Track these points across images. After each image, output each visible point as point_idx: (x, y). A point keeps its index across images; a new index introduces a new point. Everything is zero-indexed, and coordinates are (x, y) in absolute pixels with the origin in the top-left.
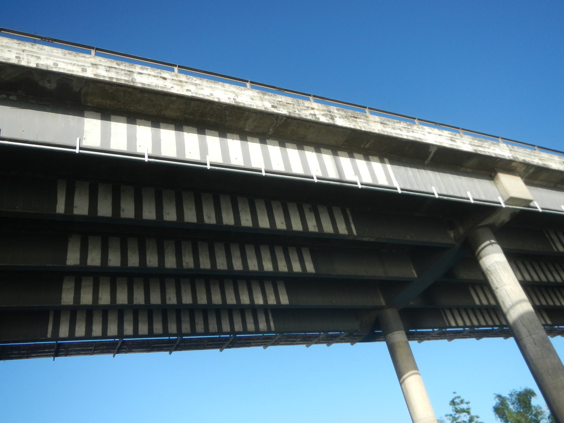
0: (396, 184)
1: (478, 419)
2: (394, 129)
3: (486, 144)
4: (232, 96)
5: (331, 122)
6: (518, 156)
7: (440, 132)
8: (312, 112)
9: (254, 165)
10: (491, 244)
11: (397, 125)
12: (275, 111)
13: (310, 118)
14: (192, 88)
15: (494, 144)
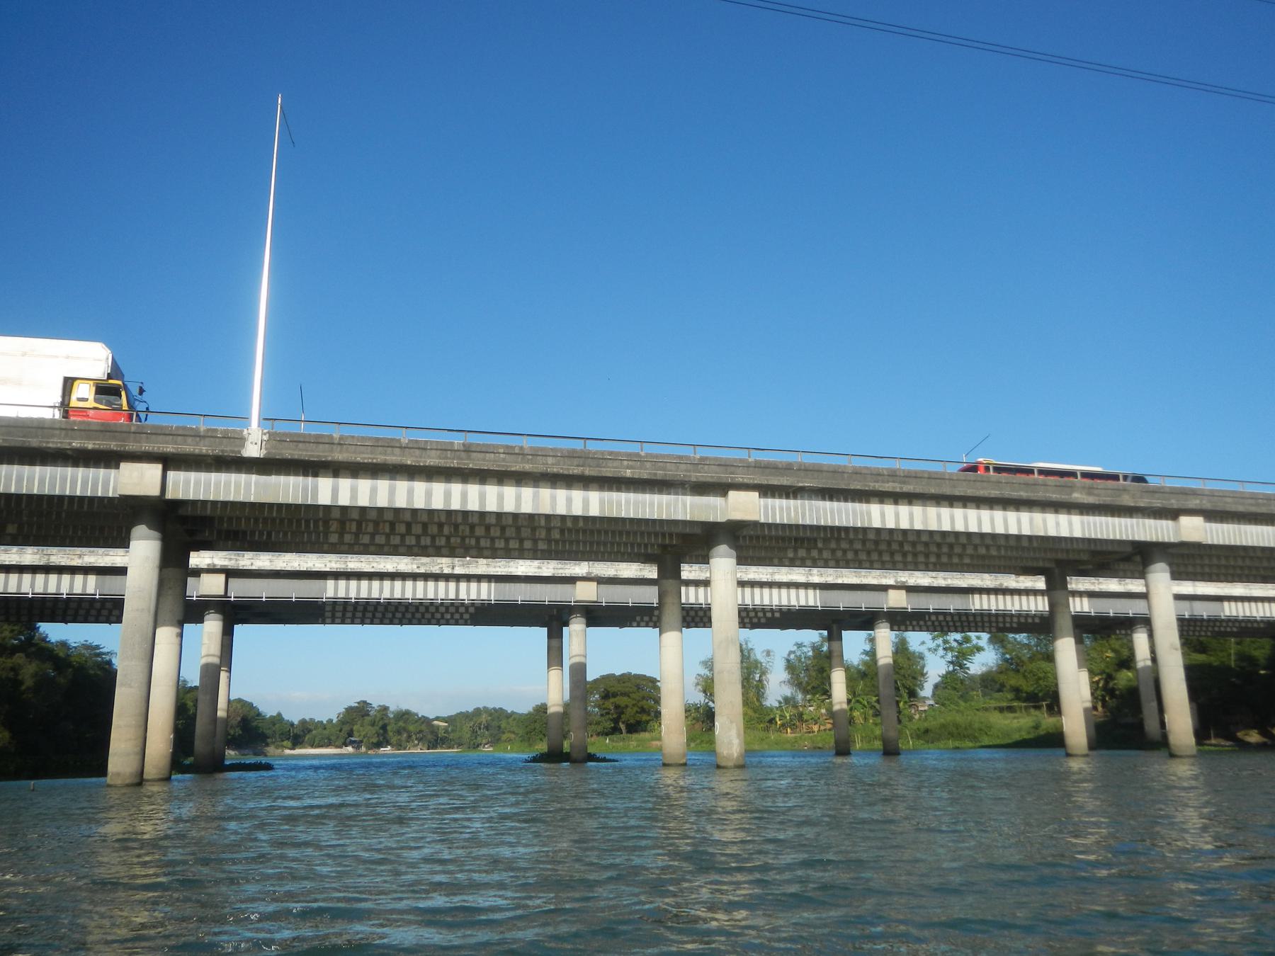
0: (492, 598)
1: (979, 641)
2: (495, 567)
3: (568, 566)
4: (395, 565)
5: (450, 572)
6: (594, 571)
7: (531, 564)
8: (441, 566)
9: (406, 597)
10: (576, 617)
11: (498, 564)
12: (418, 571)
13: (437, 572)
14: (375, 565)
15: (575, 564)
